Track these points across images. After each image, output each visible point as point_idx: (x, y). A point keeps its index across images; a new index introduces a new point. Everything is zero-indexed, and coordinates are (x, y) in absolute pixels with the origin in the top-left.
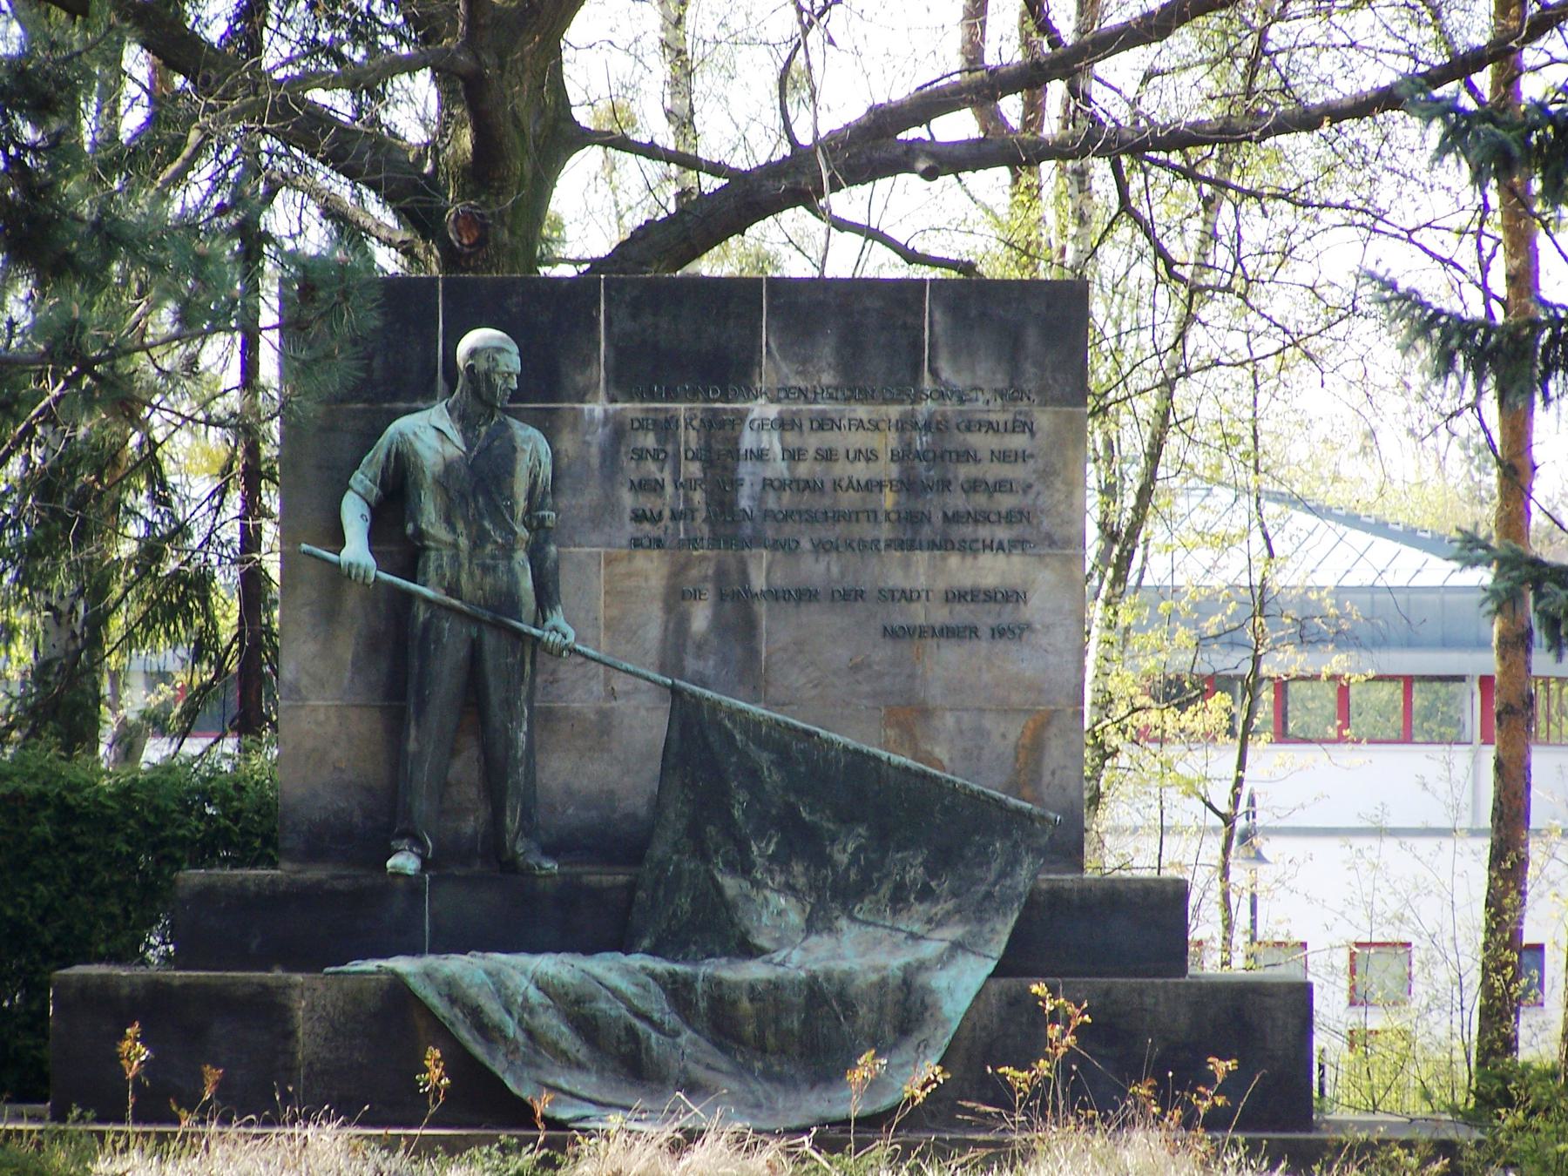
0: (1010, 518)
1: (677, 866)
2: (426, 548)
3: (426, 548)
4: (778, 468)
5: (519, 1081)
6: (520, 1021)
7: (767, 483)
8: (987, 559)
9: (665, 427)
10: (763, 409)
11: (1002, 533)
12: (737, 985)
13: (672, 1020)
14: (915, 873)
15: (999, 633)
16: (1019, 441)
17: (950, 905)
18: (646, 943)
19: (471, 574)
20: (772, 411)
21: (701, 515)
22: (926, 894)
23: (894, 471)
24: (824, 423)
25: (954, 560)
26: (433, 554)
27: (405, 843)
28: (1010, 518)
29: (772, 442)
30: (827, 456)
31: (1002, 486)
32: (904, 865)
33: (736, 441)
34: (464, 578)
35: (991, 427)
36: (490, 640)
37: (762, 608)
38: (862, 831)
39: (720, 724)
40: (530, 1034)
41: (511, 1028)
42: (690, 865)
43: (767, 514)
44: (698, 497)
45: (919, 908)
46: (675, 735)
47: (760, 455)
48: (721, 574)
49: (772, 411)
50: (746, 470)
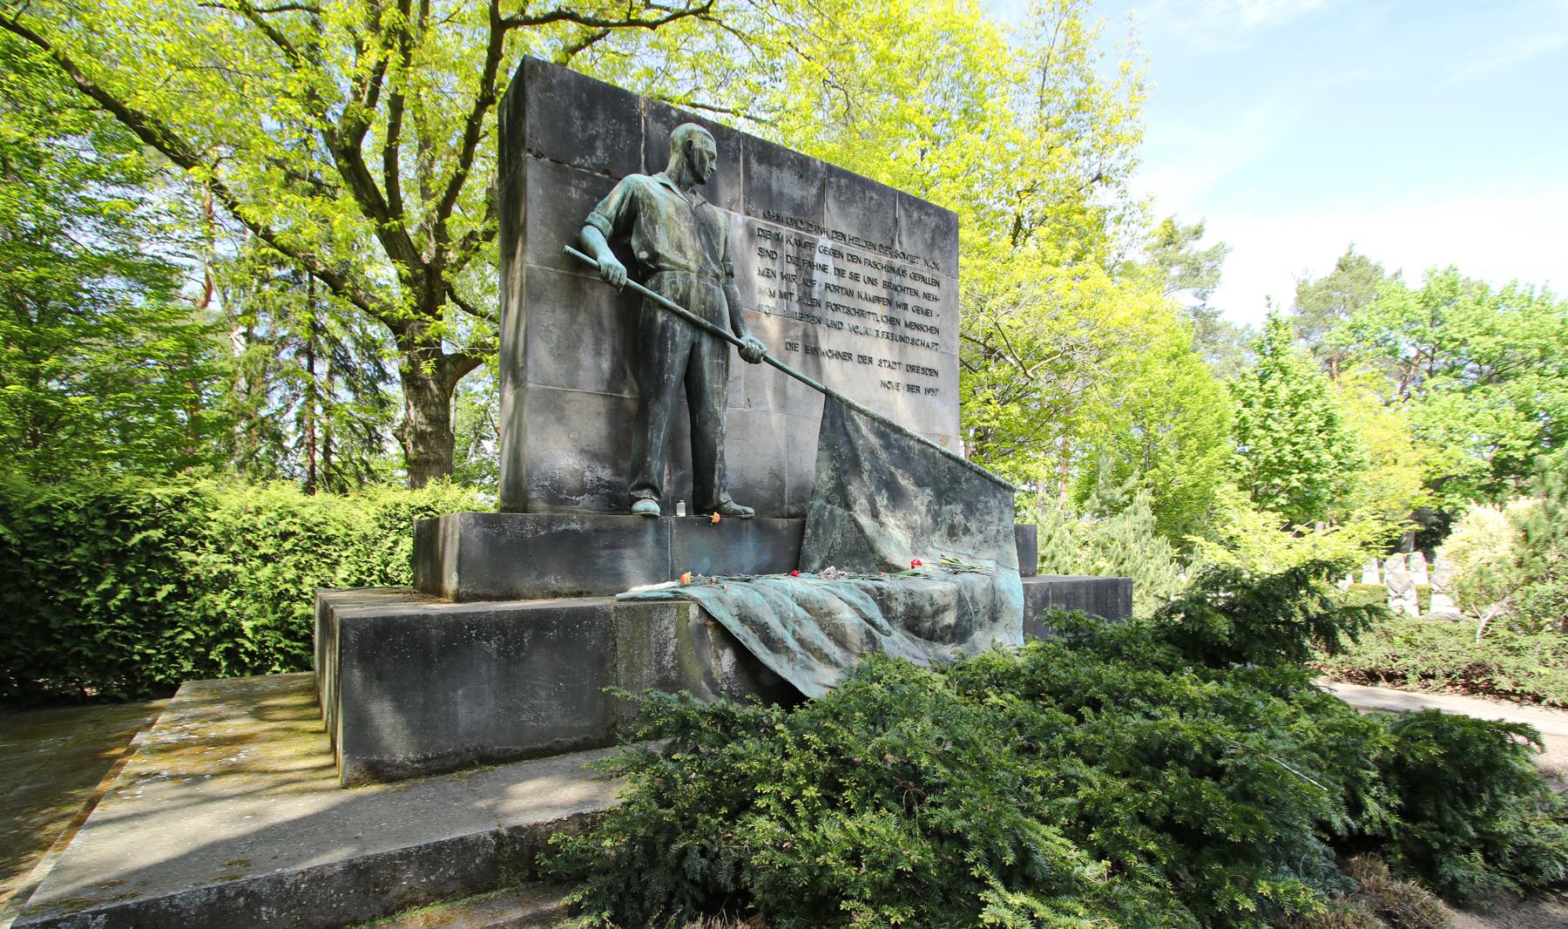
0: (934, 330)
1: (831, 512)
2: (661, 269)
3: (661, 269)
4: (832, 279)
5: (805, 683)
6: (794, 632)
7: (827, 286)
8: (922, 351)
9: (777, 239)
10: (823, 241)
11: (928, 338)
12: (922, 595)
13: (886, 625)
14: (959, 519)
15: (928, 391)
16: (933, 290)
17: (980, 537)
18: (816, 565)
19: (699, 291)
20: (829, 244)
21: (795, 298)
22: (967, 531)
23: (884, 294)
24: (853, 258)
25: (910, 347)
26: (666, 274)
27: (646, 493)
28: (934, 330)
29: (829, 261)
30: (855, 277)
31: (927, 313)
32: (952, 513)
33: (812, 257)
34: (693, 293)
35: (924, 279)
36: (706, 346)
37: (825, 361)
38: (928, 491)
39: (853, 420)
40: (802, 642)
41: (792, 643)
42: (839, 511)
43: (828, 305)
44: (794, 286)
45: (966, 539)
46: (827, 424)
47: (824, 269)
48: (805, 335)
49: (829, 244)
50: (817, 275)
